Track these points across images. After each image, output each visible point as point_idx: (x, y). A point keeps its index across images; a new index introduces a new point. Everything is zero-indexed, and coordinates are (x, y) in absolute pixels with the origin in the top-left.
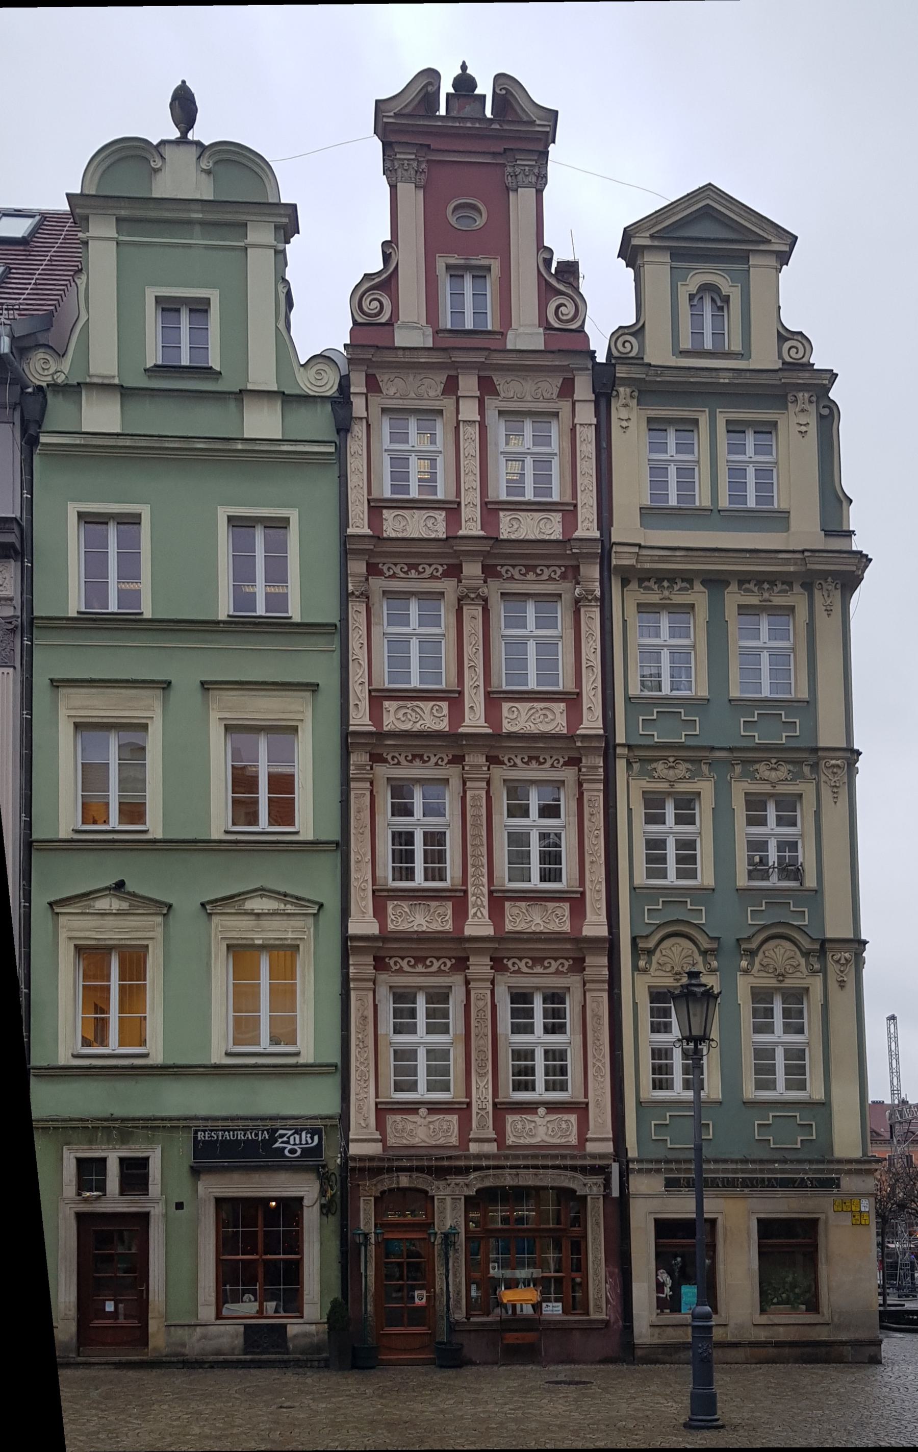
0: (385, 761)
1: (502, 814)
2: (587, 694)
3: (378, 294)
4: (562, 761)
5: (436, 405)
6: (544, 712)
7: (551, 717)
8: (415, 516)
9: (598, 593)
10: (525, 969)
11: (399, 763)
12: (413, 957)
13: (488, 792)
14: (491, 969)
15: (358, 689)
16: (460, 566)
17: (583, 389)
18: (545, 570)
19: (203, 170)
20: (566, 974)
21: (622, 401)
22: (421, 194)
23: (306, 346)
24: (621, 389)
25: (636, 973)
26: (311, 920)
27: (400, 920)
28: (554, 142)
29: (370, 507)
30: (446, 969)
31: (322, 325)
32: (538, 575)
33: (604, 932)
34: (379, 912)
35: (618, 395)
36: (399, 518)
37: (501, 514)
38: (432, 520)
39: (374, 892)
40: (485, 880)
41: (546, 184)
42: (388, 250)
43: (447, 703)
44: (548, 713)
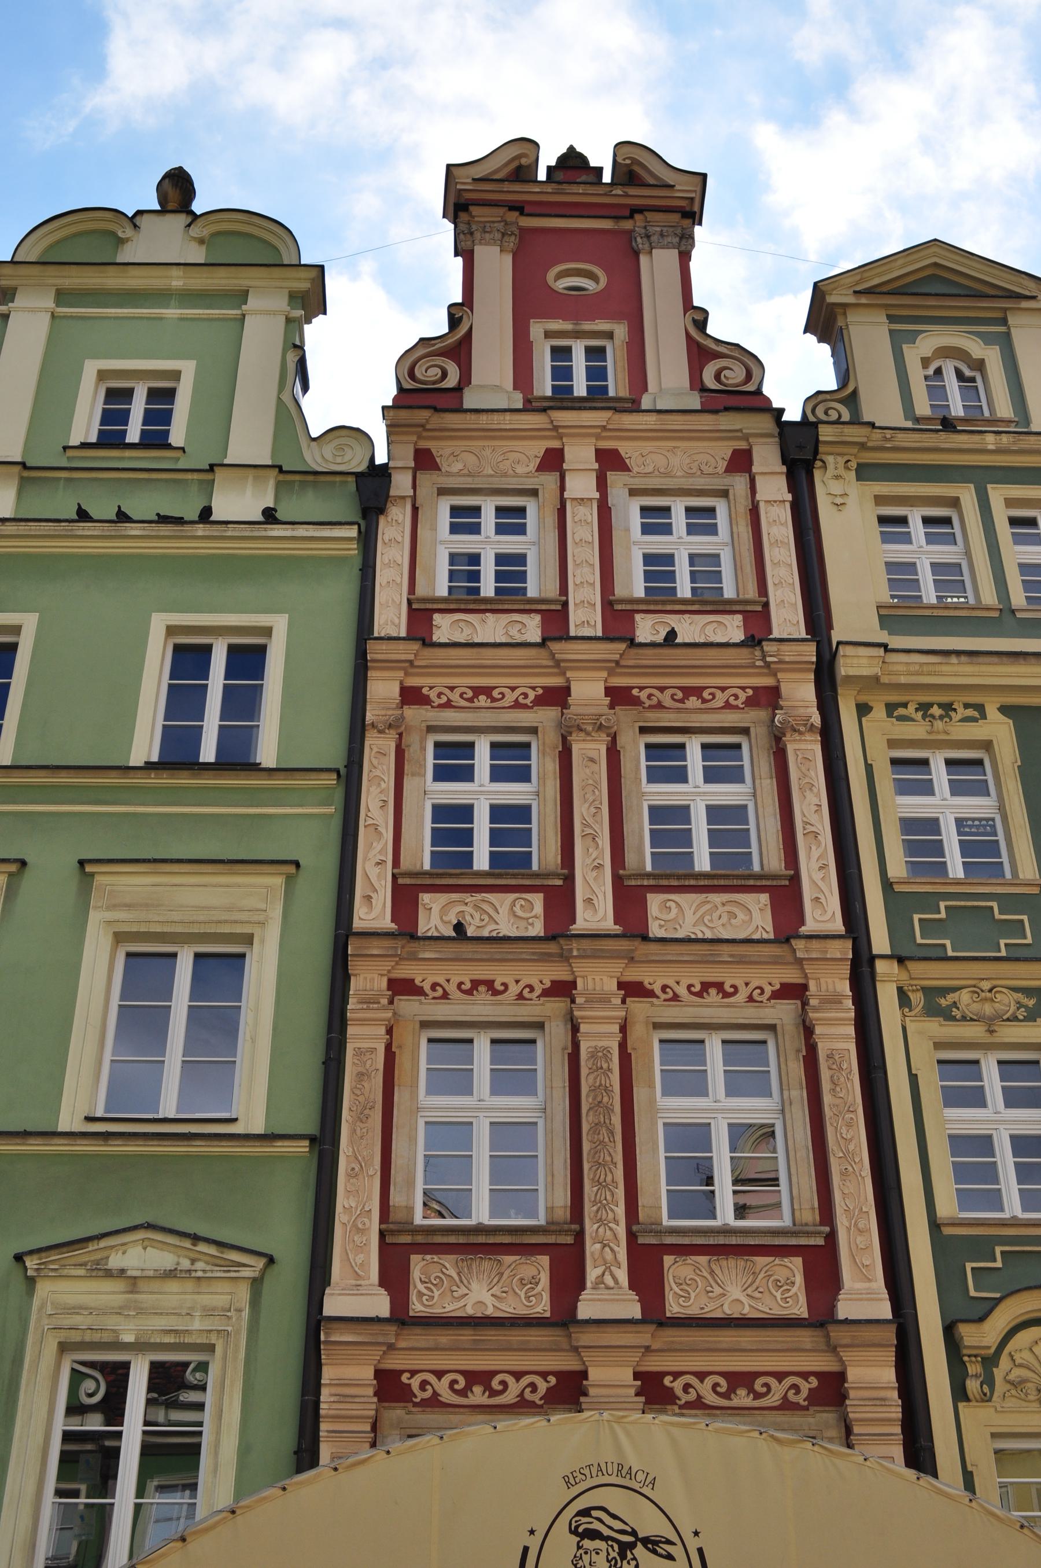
0: (419, 992)
1: (651, 1085)
2: (810, 877)
3: (439, 361)
4: (768, 990)
5: (529, 484)
6: (727, 908)
7: (741, 916)
8: (487, 621)
9: (816, 719)
10: (711, 1399)
11: (445, 996)
12: (462, 1373)
13: (623, 1046)
14: (637, 1395)
15: (373, 872)
16: (566, 691)
17: (767, 459)
18: (718, 693)
19: (194, 239)
20: (806, 1408)
21: (831, 471)
22: (508, 260)
23: (320, 412)
24: (830, 460)
25: (961, 1405)
26: (243, 1294)
27: (437, 1293)
28: (700, 224)
29: (411, 611)
30: (536, 1398)
31: (350, 383)
32: (704, 701)
33: (884, 1310)
34: (394, 1276)
35: (825, 467)
36: (462, 624)
37: (638, 617)
38: (519, 626)
39: (382, 1234)
40: (621, 1211)
41: (693, 245)
42: (455, 316)
43: (541, 896)
44: (735, 910)
